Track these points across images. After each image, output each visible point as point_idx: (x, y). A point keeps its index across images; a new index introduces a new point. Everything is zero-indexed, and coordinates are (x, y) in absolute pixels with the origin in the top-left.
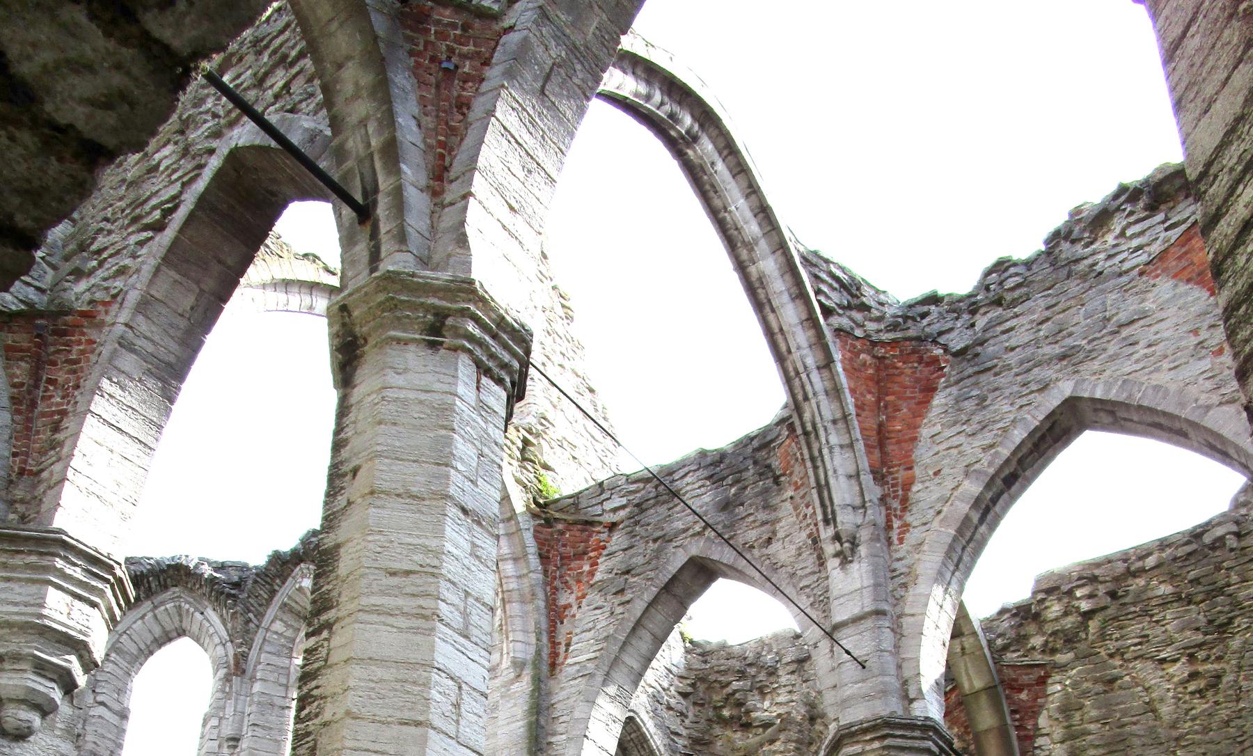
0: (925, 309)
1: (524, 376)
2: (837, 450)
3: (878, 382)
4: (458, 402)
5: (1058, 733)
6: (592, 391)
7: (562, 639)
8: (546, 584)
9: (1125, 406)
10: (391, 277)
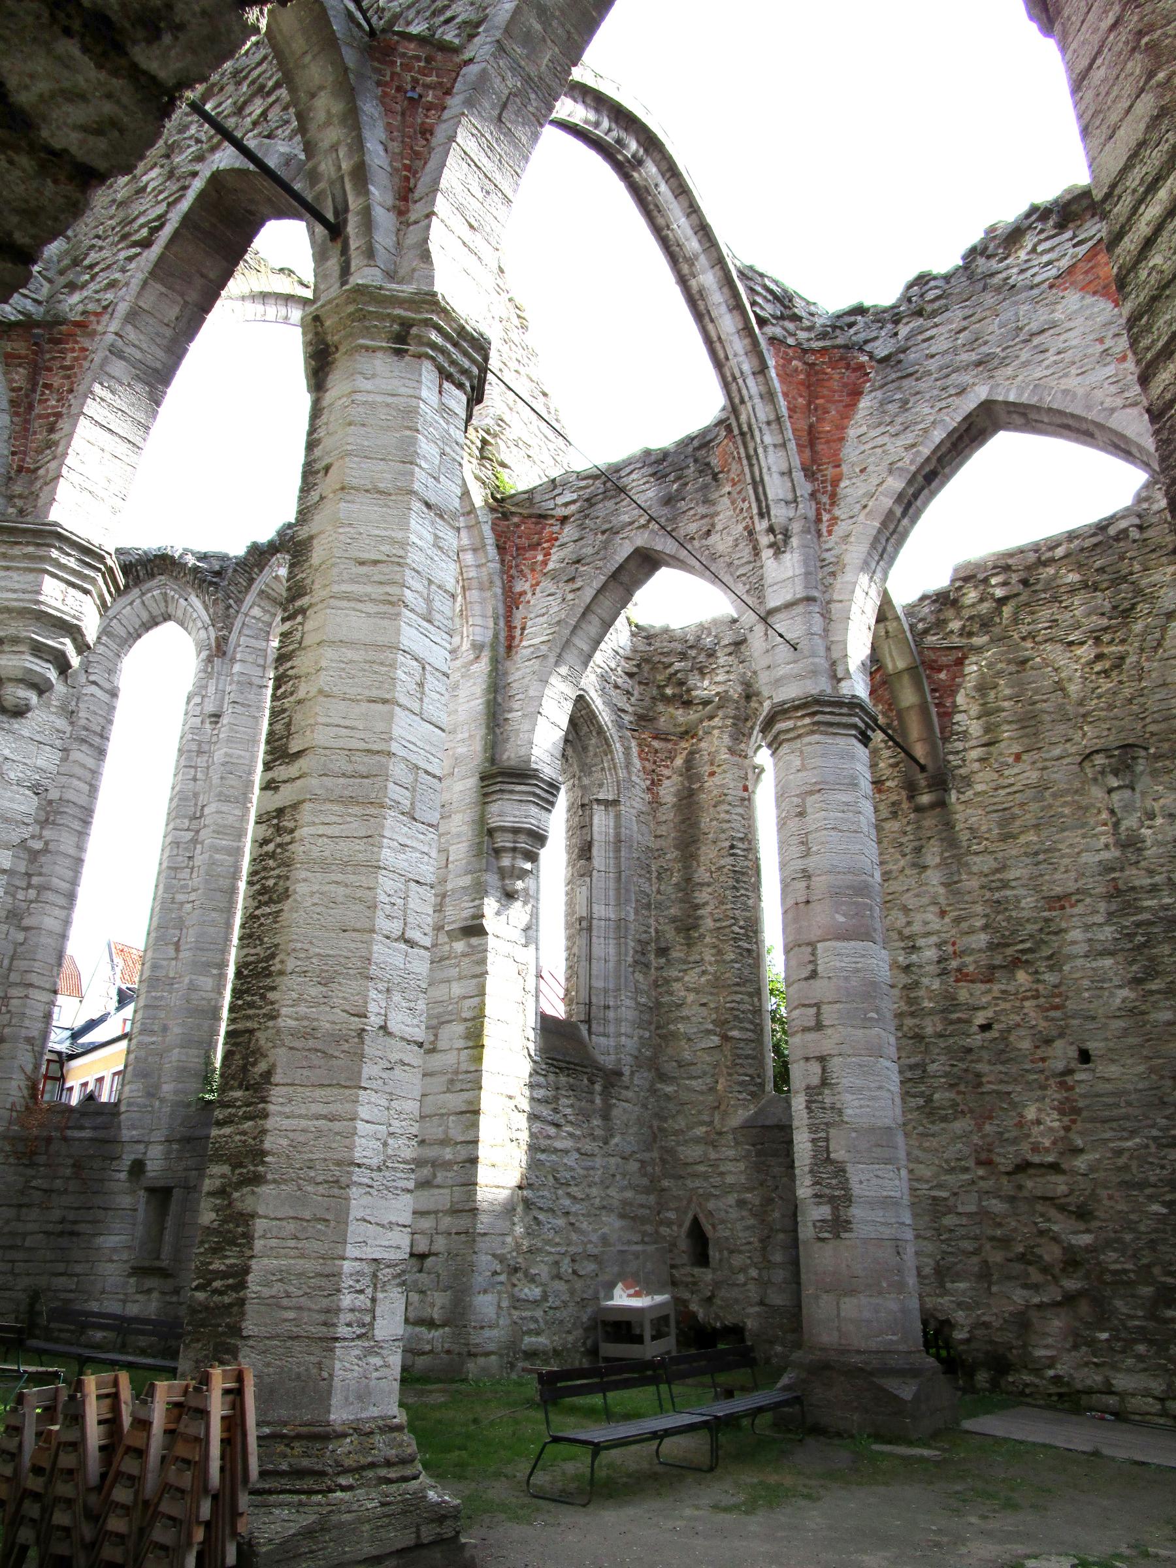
0: (852, 319)
1: (482, 381)
2: (771, 449)
3: (808, 387)
4: (422, 405)
5: (975, 709)
6: (545, 395)
7: (517, 623)
8: (502, 572)
9: (1037, 408)
10: (360, 290)
